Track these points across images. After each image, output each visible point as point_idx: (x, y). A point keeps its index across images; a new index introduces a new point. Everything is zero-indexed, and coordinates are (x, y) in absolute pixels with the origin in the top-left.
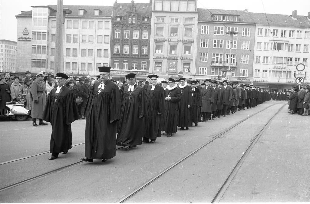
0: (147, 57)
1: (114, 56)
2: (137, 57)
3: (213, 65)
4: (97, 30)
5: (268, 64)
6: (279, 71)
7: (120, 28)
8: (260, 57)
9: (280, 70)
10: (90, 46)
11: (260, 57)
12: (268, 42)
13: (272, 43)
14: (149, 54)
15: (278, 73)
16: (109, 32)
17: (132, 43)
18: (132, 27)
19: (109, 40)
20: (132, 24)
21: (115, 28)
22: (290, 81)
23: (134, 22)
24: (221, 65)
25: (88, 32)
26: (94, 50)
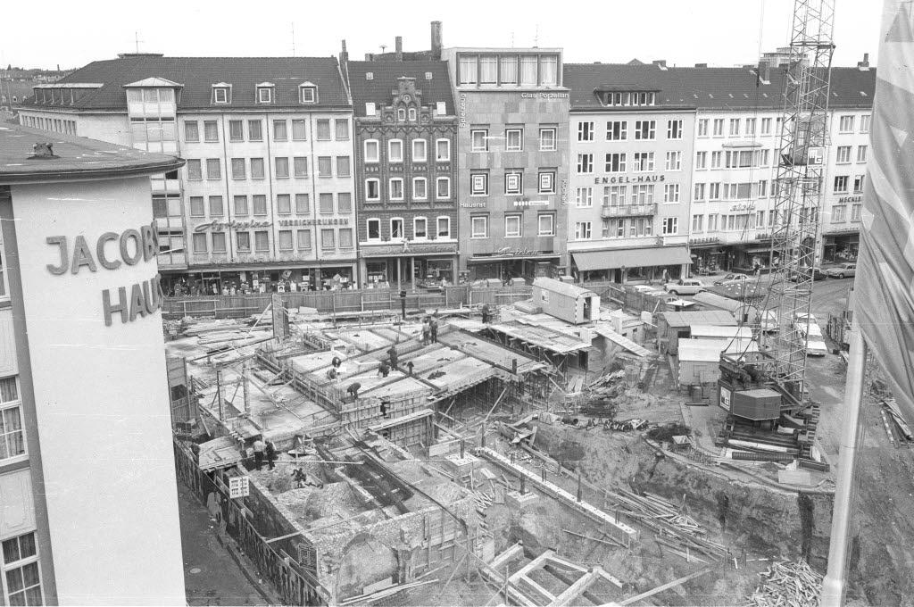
0: (450, 207)
1: (366, 209)
3: (607, 214)
4: (315, 143)
5: (720, 201)
6: (743, 215)
7: (378, 134)
8: (703, 185)
9: (746, 212)
10: (303, 187)
11: (703, 185)
12: (720, 149)
13: (728, 152)
15: (741, 219)
18: (407, 131)
20: (407, 126)
22: (762, 232)
23: (413, 120)
24: (622, 213)
25: (290, 149)
26: (311, 196)
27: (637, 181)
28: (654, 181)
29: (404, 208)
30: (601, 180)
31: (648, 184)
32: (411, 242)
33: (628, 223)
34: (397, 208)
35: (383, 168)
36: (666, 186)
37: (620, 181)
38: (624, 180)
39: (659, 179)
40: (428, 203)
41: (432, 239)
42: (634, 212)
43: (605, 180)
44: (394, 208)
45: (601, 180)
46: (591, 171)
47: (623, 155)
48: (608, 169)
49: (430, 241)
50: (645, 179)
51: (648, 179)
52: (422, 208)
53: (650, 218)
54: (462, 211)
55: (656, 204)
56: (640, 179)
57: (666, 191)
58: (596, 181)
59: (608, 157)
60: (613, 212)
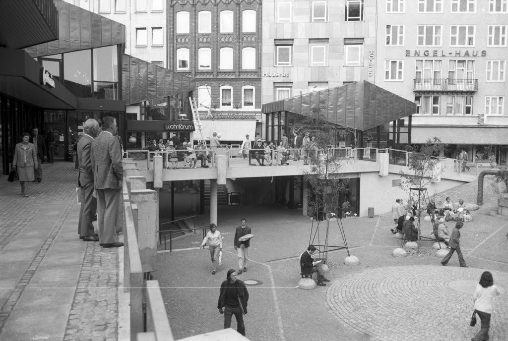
0: (256, 77)
2: (208, 77)
4: (133, 16)
14: (260, 68)
16: (162, 20)
17: (216, 41)
19: (160, 37)
21: (177, 7)
27: (454, 54)
28: (475, 56)
29: (212, 77)
30: (412, 54)
31: (467, 59)
32: (217, 110)
33: (444, 101)
34: (204, 77)
35: (194, 41)
36: (489, 63)
37: (435, 53)
38: (439, 54)
39: (480, 54)
40: (233, 72)
41: (237, 108)
42: (451, 88)
43: (417, 54)
44: (202, 77)
45: (412, 54)
46: (401, 42)
47: (438, 28)
48: (421, 42)
49: (235, 110)
50: (463, 54)
51: (467, 54)
52: (227, 77)
53: (471, 93)
54: (264, 80)
55: (476, 80)
56: (458, 54)
57: (489, 68)
58: (408, 54)
59: (421, 28)
60: (428, 87)
